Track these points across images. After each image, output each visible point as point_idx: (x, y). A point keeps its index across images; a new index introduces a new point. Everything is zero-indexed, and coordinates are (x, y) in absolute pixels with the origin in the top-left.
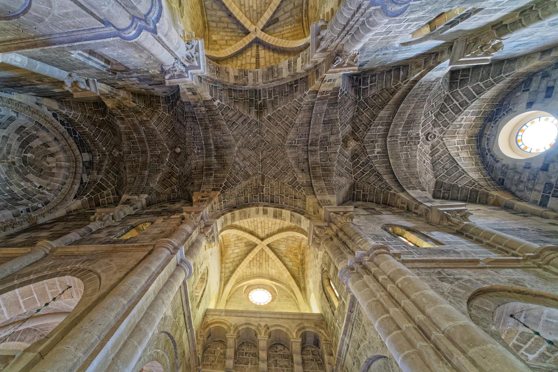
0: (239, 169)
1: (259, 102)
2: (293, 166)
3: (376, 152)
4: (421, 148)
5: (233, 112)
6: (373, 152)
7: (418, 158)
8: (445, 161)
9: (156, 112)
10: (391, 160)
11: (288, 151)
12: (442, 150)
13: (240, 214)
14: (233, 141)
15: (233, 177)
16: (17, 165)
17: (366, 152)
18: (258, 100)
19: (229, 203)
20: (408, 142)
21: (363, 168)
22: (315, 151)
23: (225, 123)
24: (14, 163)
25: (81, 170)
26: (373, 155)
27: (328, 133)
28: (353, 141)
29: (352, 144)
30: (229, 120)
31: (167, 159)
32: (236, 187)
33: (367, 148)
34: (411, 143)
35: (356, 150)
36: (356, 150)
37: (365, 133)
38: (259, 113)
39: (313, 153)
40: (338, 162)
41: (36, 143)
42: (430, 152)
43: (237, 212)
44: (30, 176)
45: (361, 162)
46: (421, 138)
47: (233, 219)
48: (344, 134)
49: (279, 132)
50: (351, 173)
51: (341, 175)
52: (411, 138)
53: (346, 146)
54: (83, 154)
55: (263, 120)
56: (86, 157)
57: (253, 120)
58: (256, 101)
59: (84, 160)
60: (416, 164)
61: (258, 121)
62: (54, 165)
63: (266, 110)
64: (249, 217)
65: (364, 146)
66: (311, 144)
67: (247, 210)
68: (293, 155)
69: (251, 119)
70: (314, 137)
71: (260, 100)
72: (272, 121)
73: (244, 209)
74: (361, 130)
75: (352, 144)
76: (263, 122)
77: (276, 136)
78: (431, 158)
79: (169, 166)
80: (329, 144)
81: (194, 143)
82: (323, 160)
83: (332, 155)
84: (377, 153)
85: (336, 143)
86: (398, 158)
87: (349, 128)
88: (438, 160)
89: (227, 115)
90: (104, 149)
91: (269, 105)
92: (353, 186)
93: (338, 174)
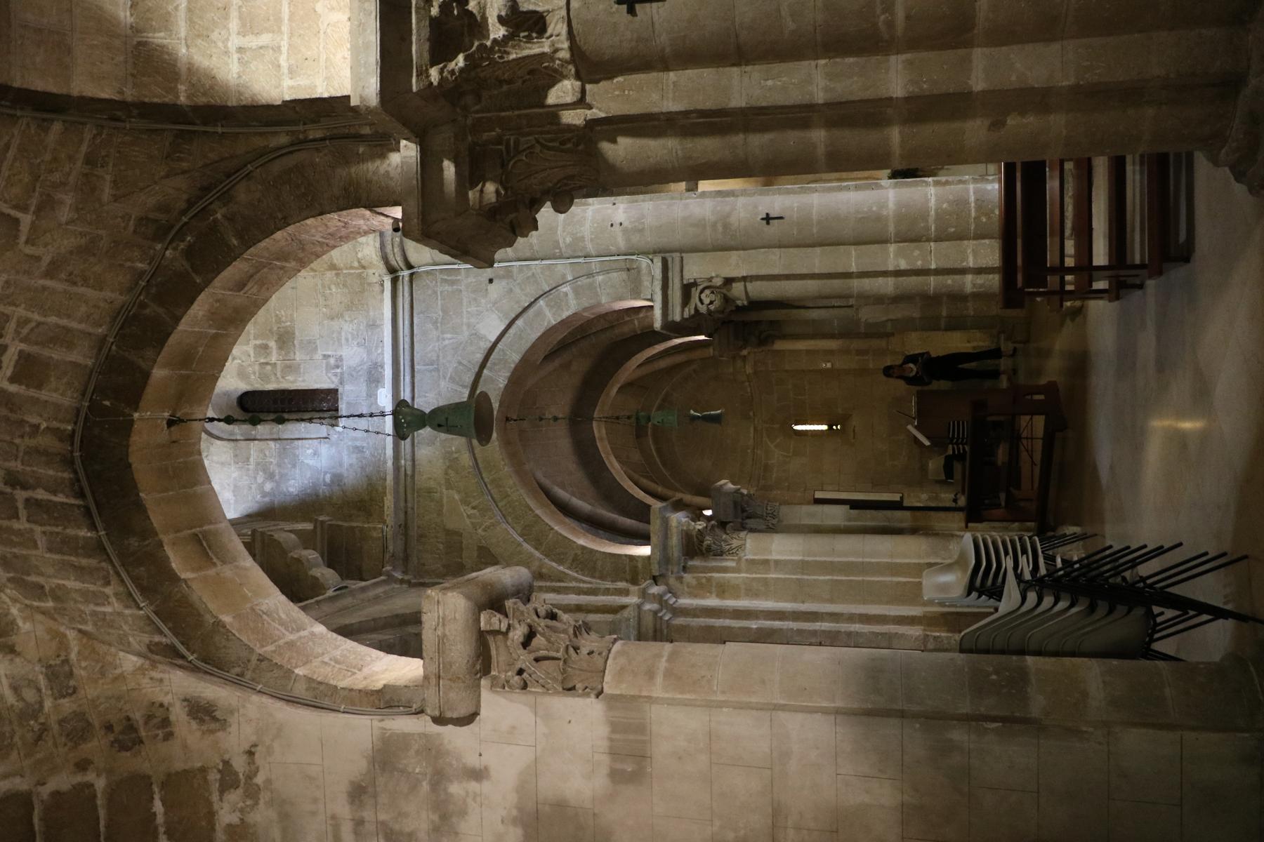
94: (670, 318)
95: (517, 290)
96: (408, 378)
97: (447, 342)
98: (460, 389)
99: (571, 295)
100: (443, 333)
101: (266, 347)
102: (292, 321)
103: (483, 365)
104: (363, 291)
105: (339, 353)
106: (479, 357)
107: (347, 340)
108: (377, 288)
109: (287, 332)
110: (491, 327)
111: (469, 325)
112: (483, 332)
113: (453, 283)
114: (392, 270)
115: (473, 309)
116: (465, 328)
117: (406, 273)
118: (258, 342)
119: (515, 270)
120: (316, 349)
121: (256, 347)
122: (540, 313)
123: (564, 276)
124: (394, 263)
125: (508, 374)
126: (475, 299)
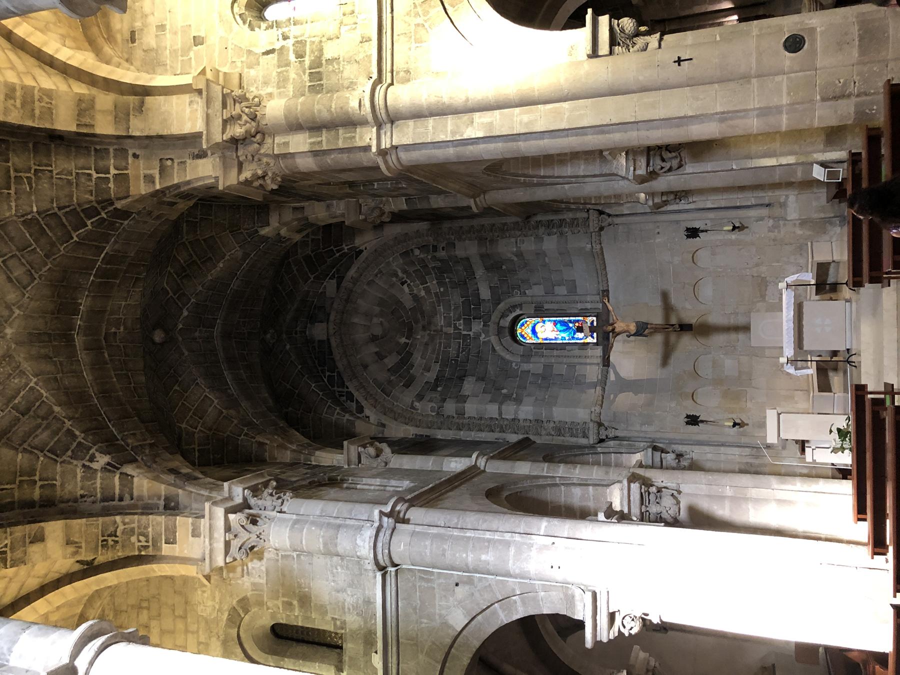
0: (10, 263)
5: (37, 441)
9: (210, 429)
13: (49, 112)
15: (43, 241)
16: (420, 325)
19: (81, 162)
23: (57, 409)
24: (424, 328)
25: (335, 306)
30: (43, 419)
31: (185, 313)
32: (45, 205)
41: (391, 360)
43: (65, 122)
44: (409, 303)
47: (84, 107)
54: (325, 338)
56: (318, 331)
59: (324, 325)
62: (375, 320)
73: (29, 123)
79: (184, 294)
81: (126, 355)
90: (288, 347)
94: (598, 639)
95: (477, 595)
96: (394, 649)
97: (423, 625)
98: (433, 663)
99: (519, 603)
100: (421, 617)
101: (291, 604)
102: (310, 588)
103: (451, 646)
104: (361, 574)
105: (344, 618)
106: (449, 641)
107: (349, 609)
108: (371, 574)
109: (306, 596)
110: (458, 620)
111: (440, 615)
112: (451, 622)
113: (428, 581)
114: (382, 568)
115: (443, 603)
116: (437, 617)
117: (393, 569)
118: (286, 599)
119: (476, 580)
120: (326, 612)
121: (283, 602)
122: (495, 613)
123: (514, 590)
124: (382, 563)
125: (471, 656)
126: (445, 596)
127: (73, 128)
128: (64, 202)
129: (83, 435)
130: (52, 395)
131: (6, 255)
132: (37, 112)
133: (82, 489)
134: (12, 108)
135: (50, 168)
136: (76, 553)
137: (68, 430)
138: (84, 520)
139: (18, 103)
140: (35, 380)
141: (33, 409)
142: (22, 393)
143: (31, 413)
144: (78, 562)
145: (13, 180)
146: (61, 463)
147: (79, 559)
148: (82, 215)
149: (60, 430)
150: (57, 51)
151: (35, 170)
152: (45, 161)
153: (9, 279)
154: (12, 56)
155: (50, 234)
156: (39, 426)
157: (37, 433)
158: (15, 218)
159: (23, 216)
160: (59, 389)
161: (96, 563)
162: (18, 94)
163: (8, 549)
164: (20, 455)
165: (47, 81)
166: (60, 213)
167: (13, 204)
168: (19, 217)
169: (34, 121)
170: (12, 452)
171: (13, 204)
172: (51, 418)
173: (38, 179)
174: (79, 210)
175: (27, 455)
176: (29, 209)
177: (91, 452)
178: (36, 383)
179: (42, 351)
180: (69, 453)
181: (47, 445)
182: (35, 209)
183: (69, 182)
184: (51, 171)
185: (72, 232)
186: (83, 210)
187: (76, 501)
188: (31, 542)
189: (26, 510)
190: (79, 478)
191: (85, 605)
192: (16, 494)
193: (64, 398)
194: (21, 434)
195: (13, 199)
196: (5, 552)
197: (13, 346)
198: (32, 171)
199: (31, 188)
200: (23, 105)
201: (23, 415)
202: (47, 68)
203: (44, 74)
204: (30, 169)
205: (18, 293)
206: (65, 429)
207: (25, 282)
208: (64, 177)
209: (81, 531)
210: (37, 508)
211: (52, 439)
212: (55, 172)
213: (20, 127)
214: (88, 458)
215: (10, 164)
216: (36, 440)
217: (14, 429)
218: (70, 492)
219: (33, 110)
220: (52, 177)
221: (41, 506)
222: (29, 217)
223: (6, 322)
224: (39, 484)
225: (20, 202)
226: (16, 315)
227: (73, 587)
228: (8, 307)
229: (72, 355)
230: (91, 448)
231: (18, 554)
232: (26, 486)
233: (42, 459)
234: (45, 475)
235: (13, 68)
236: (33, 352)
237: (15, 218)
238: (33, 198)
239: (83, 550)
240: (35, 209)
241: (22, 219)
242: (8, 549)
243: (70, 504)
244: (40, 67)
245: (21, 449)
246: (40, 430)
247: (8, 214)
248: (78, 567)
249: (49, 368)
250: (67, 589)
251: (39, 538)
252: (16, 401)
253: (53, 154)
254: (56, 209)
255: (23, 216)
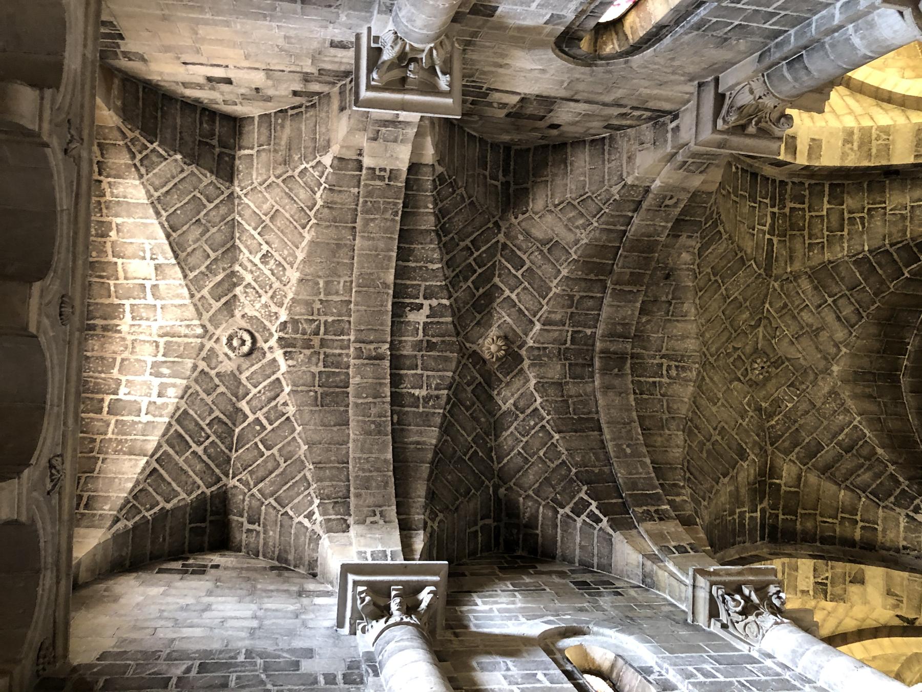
1: (765, 504)
2: (690, 295)
3: (426, 311)
4: (274, 309)
6: (433, 312)
7: (293, 275)
8: (199, 254)
10: (390, 278)
11: (691, 345)
12: (205, 292)
14: (845, 394)
15: (872, 280)
17: (453, 315)
18: (769, 511)
20: (317, 333)
21: (471, 260)
22: (611, 335)
23: (880, 451)
26: (434, 302)
27: (571, 389)
28: (487, 356)
29: (490, 345)
30: (866, 459)
32: (877, 243)
33: (451, 327)
34: (309, 328)
35: (478, 323)
36: (478, 323)
37: (457, 378)
38: (768, 472)
39: (619, 329)
40: (543, 290)
42: (238, 290)
45: (469, 283)
46: (273, 342)
48: (517, 383)
49: (714, 409)
50: (505, 246)
51: (552, 246)
52: (308, 345)
53: (510, 340)
55: (757, 451)
57: (787, 452)
58: (774, 507)
60: (310, 254)
61: (769, 448)
63: (752, 478)
64: (850, 133)
65: (458, 334)
66: (621, 358)
67: (851, 162)
68: (678, 329)
69: (793, 456)
70: (617, 382)
71: (763, 511)
72: (735, 447)
73: (866, 163)
74: (469, 389)
75: (490, 345)
76: (755, 442)
77: (720, 395)
78: (237, 268)
80: (562, 355)
82: (590, 303)
83: (558, 317)
84: (420, 307)
85: (540, 356)
86: (368, 283)
87: (506, 399)
88: (216, 260)
89: (878, 476)
91: (743, 491)
92: (513, 197)
93: (557, 252)
127: (911, 160)
128: (897, 237)
129: (907, 482)
130: (875, 436)
131: (836, 294)
132: (874, 151)
133: (905, 539)
134: (849, 151)
135: (884, 205)
136: (897, 606)
137: (891, 474)
138: (906, 574)
139: (855, 146)
140: (858, 418)
141: (856, 447)
142: (846, 430)
143: (854, 451)
144: (897, 616)
145: (846, 222)
146: (883, 507)
147: (899, 613)
148: (915, 249)
149: (882, 473)
150: (896, 85)
151: (869, 209)
152: (878, 199)
153: (838, 318)
154: (850, 101)
155: (880, 272)
156: (862, 466)
157: (859, 472)
158: (846, 258)
159: (853, 256)
160: (882, 430)
161: (917, 623)
162: (856, 137)
163: (828, 582)
164: (843, 491)
165: (885, 117)
166: (891, 250)
167: (846, 245)
168: (851, 257)
169: (870, 161)
170: (834, 488)
171: (846, 245)
172: (873, 459)
173: (871, 216)
174: (912, 244)
175: (849, 493)
176: (860, 249)
177: (916, 502)
178: (860, 423)
179: (867, 390)
180: (892, 499)
181: (869, 487)
182: (866, 248)
183: (903, 217)
184: (885, 208)
185: (903, 268)
186: (916, 245)
187: (897, 550)
188: (851, 582)
189: (847, 548)
190: (902, 529)
191: (902, 665)
192: (838, 530)
193: (887, 441)
194: (844, 471)
195: (845, 241)
196: (826, 585)
197: (839, 383)
198: (866, 211)
199: (863, 228)
200: (860, 147)
201: (847, 452)
202: (885, 105)
203: (881, 111)
204: (864, 208)
205: (846, 331)
206: (888, 473)
207: (853, 321)
208: (897, 212)
209: (902, 585)
210: (857, 549)
211: (874, 481)
212: (888, 209)
213: (856, 169)
214: (912, 507)
215: (844, 207)
216: (859, 479)
217: (837, 465)
218: (892, 541)
219: (870, 149)
220: (885, 214)
221: (861, 548)
222: (860, 256)
223: (833, 359)
224: (861, 524)
225: (852, 242)
226: (842, 353)
227: (892, 642)
228: (836, 345)
229: (897, 398)
230: (915, 498)
231: (838, 590)
232: (847, 524)
233: (863, 499)
234: (866, 517)
235: (851, 112)
236: (858, 390)
237: (846, 258)
238: (865, 237)
239: (904, 605)
240: (866, 248)
241: (854, 259)
242: (828, 582)
243: (891, 553)
244: (877, 105)
245: (843, 486)
246: (862, 470)
247: (840, 255)
248: (897, 622)
249: (873, 407)
250: (886, 641)
251: (859, 580)
252: (840, 438)
253: (887, 190)
254: (888, 246)
255: (853, 256)
